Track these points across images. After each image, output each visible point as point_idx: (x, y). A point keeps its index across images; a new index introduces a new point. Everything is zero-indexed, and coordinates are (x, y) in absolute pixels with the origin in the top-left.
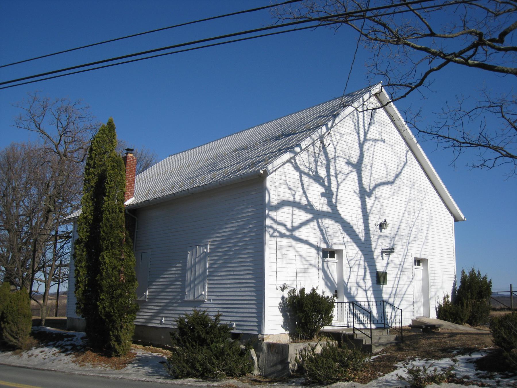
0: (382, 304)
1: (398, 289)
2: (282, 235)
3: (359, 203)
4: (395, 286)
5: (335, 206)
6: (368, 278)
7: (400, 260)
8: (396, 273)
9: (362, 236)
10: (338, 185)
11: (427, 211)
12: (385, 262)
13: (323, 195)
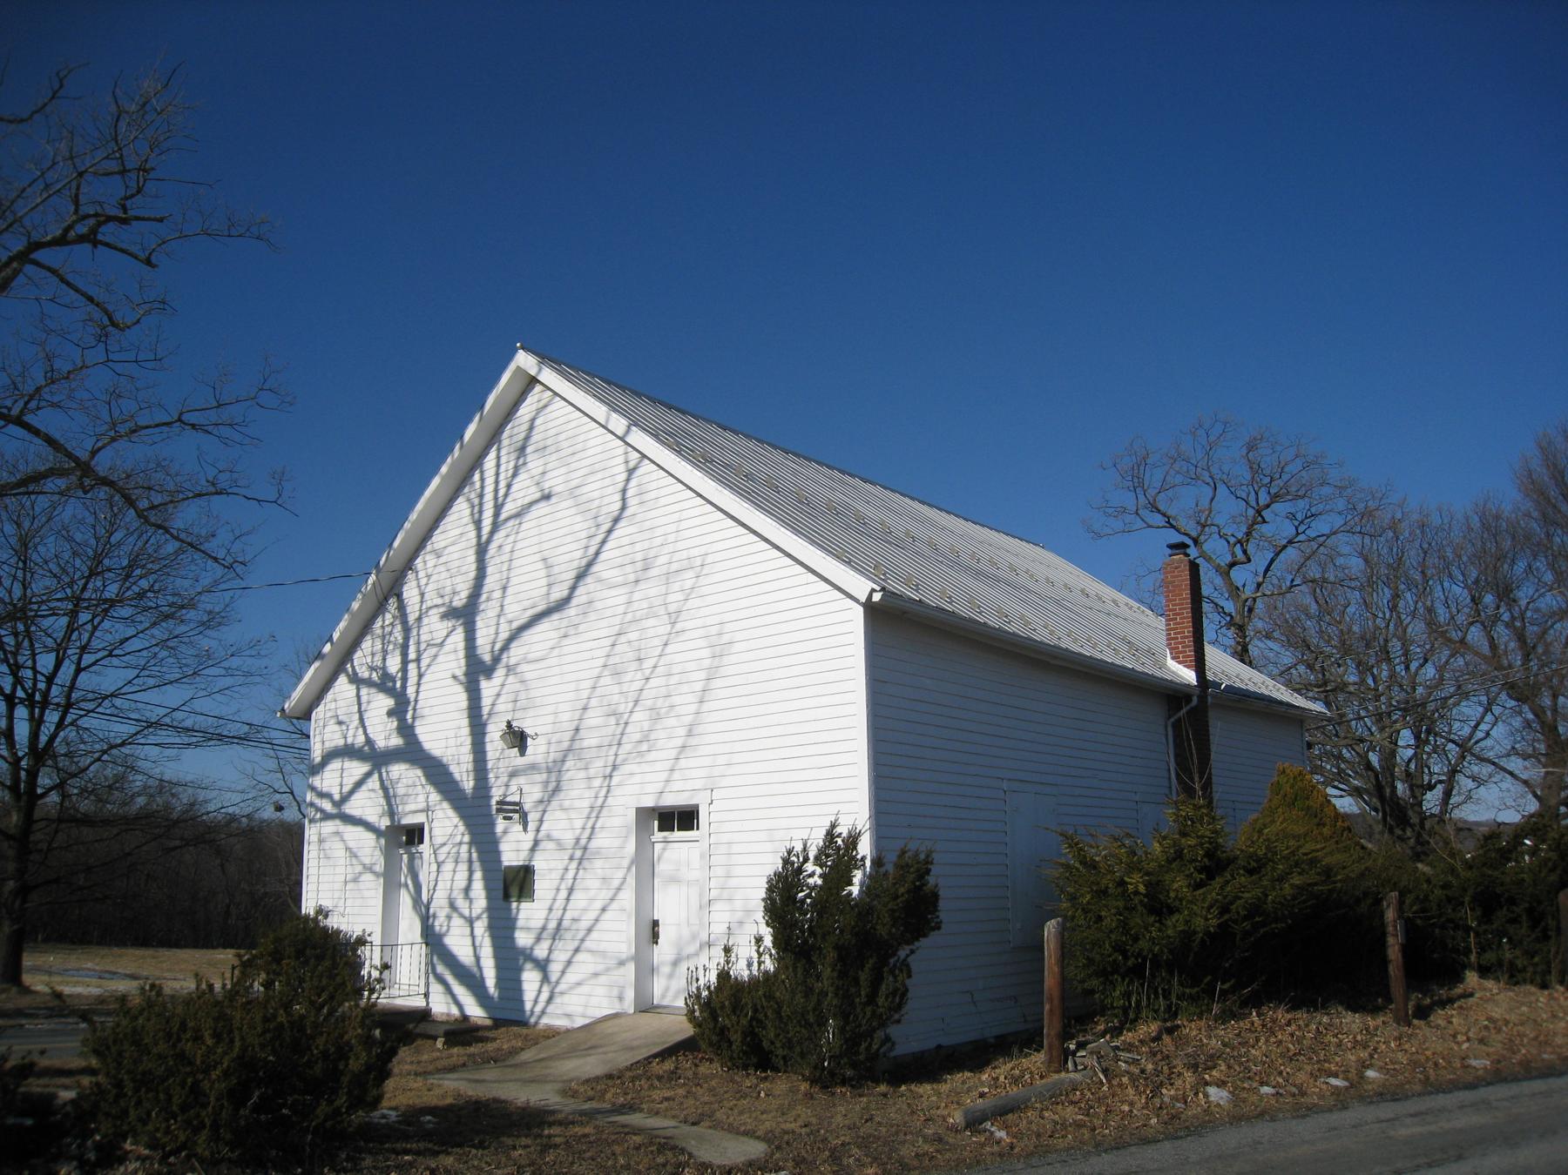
0: (510, 959)
1: (568, 915)
2: (327, 817)
3: (462, 699)
4: (560, 904)
5: (412, 727)
6: (478, 887)
7: (579, 824)
8: (561, 865)
9: (468, 784)
10: (420, 676)
11: (701, 632)
12: (531, 835)
13: (390, 713)
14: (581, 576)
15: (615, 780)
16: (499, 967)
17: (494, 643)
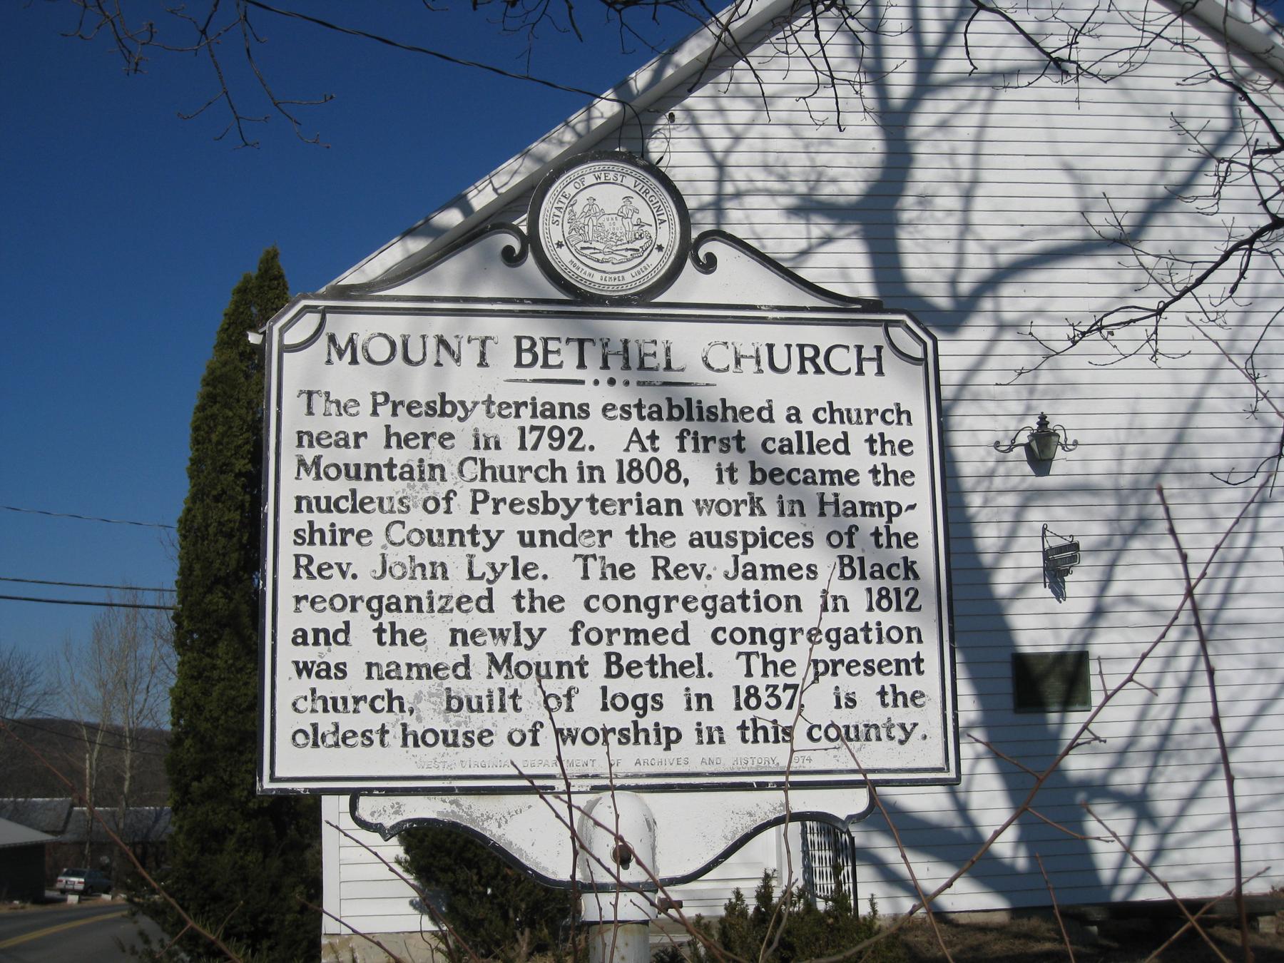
14: (1158, 206)
15: (1267, 511)
16: (1022, 814)
17: (959, 267)
